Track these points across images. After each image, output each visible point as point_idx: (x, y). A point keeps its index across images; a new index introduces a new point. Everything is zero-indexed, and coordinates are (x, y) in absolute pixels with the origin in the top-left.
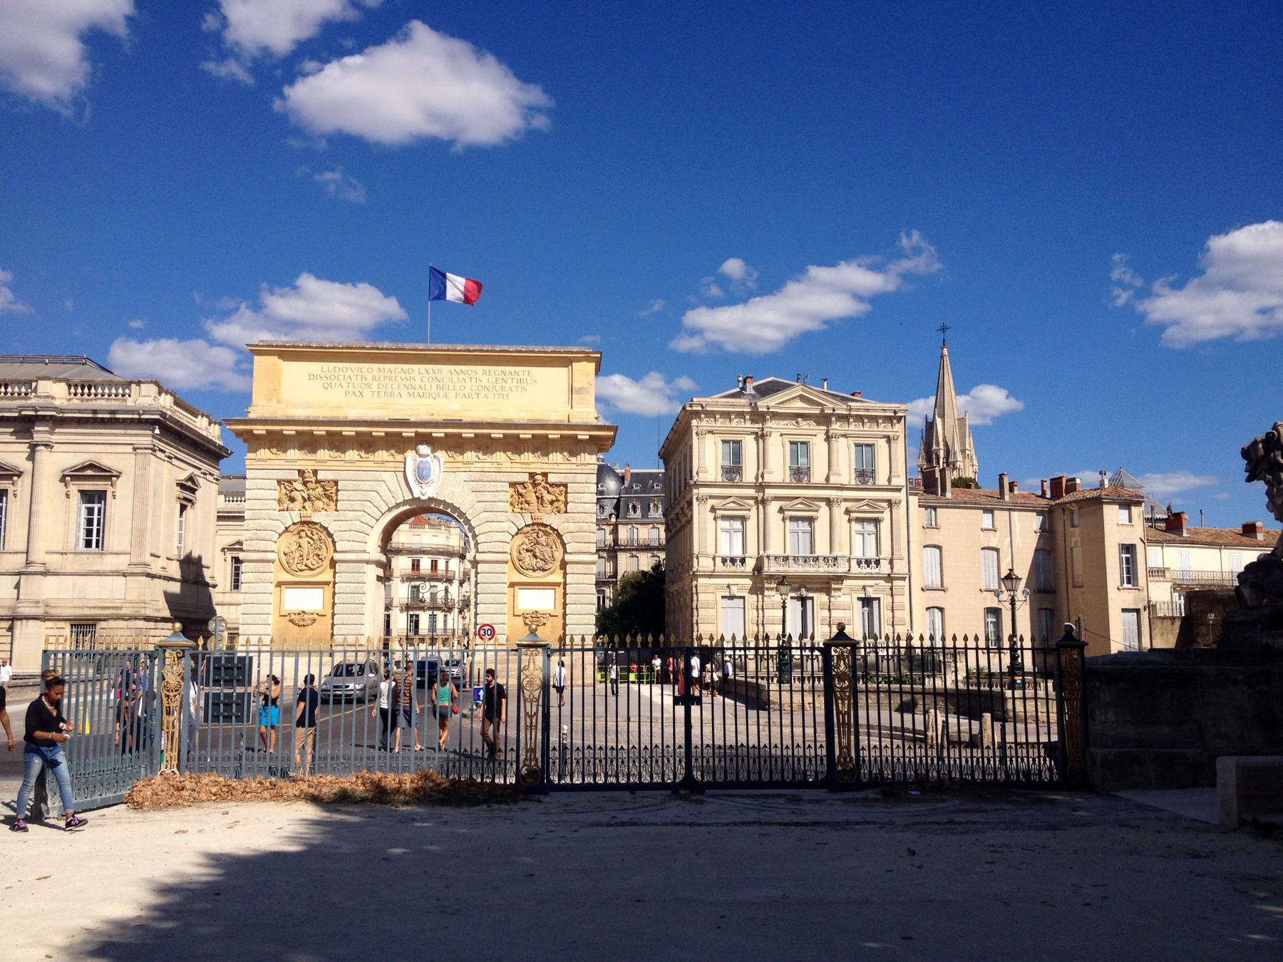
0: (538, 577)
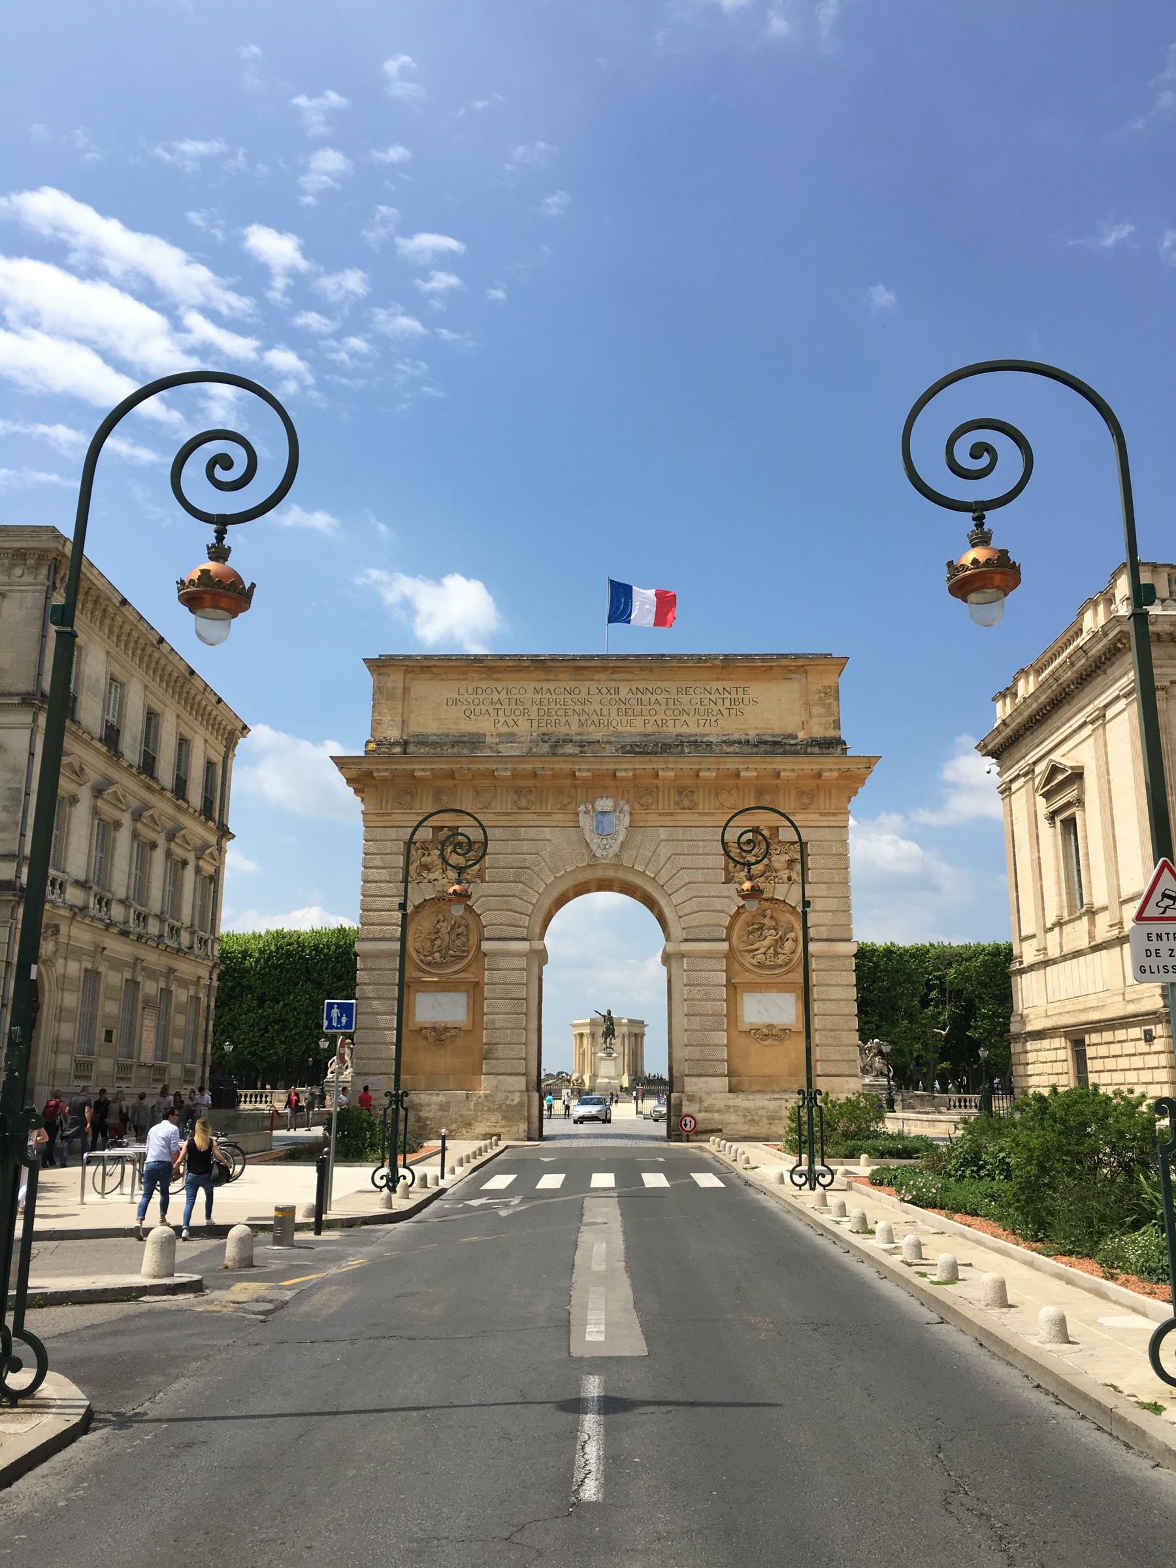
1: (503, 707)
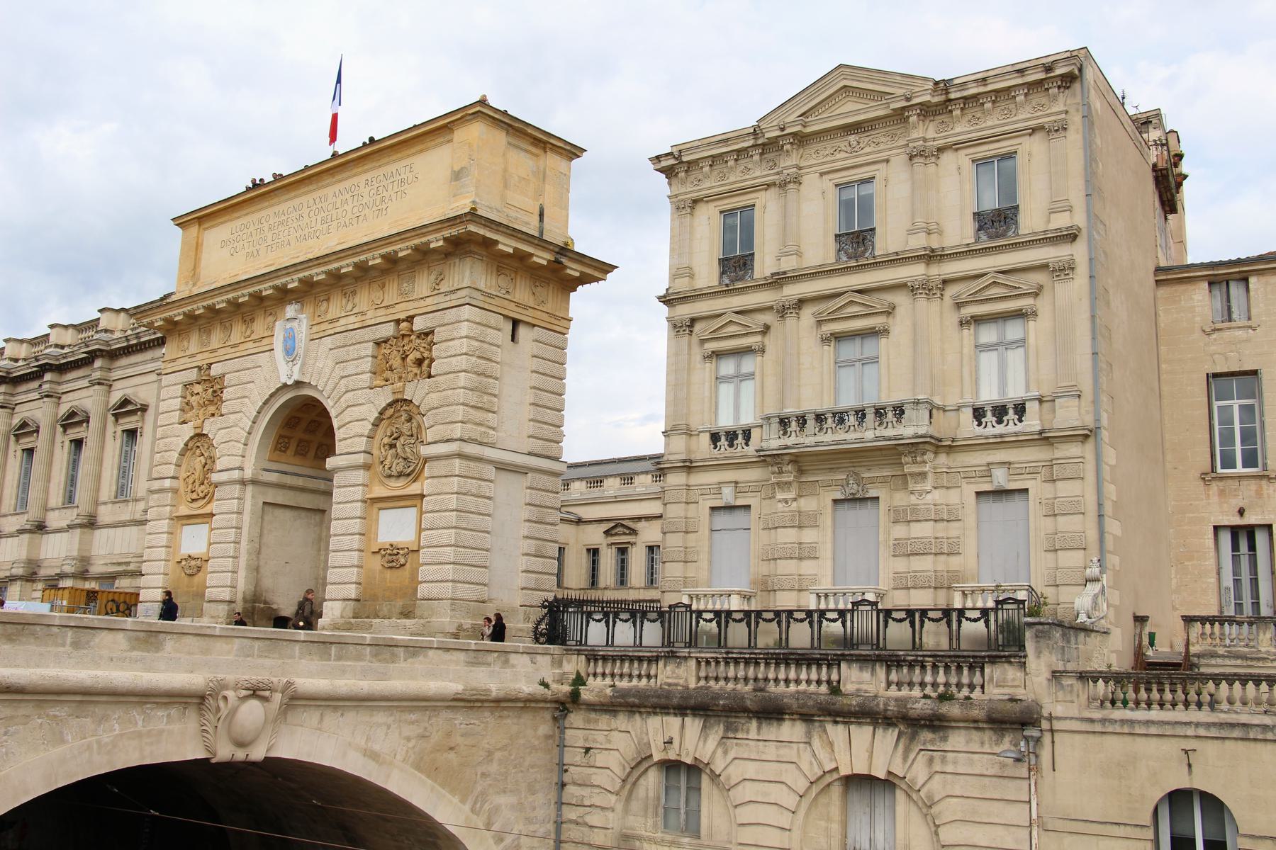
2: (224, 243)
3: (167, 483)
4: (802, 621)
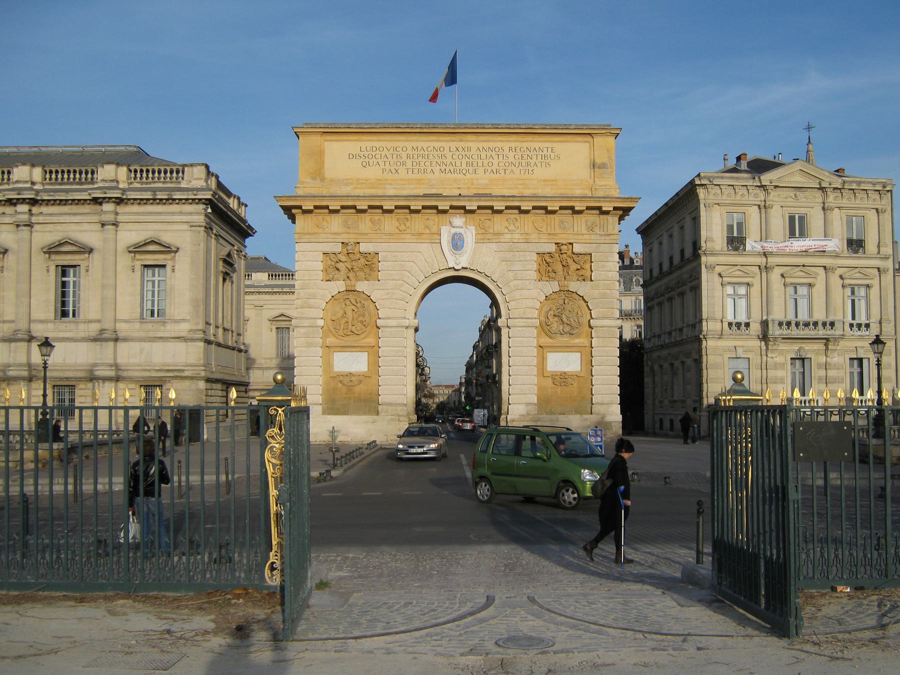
0: (565, 339)
1: (388, 160)
2: (352, 156)
3: (321, 323)
4: (850, 415)
